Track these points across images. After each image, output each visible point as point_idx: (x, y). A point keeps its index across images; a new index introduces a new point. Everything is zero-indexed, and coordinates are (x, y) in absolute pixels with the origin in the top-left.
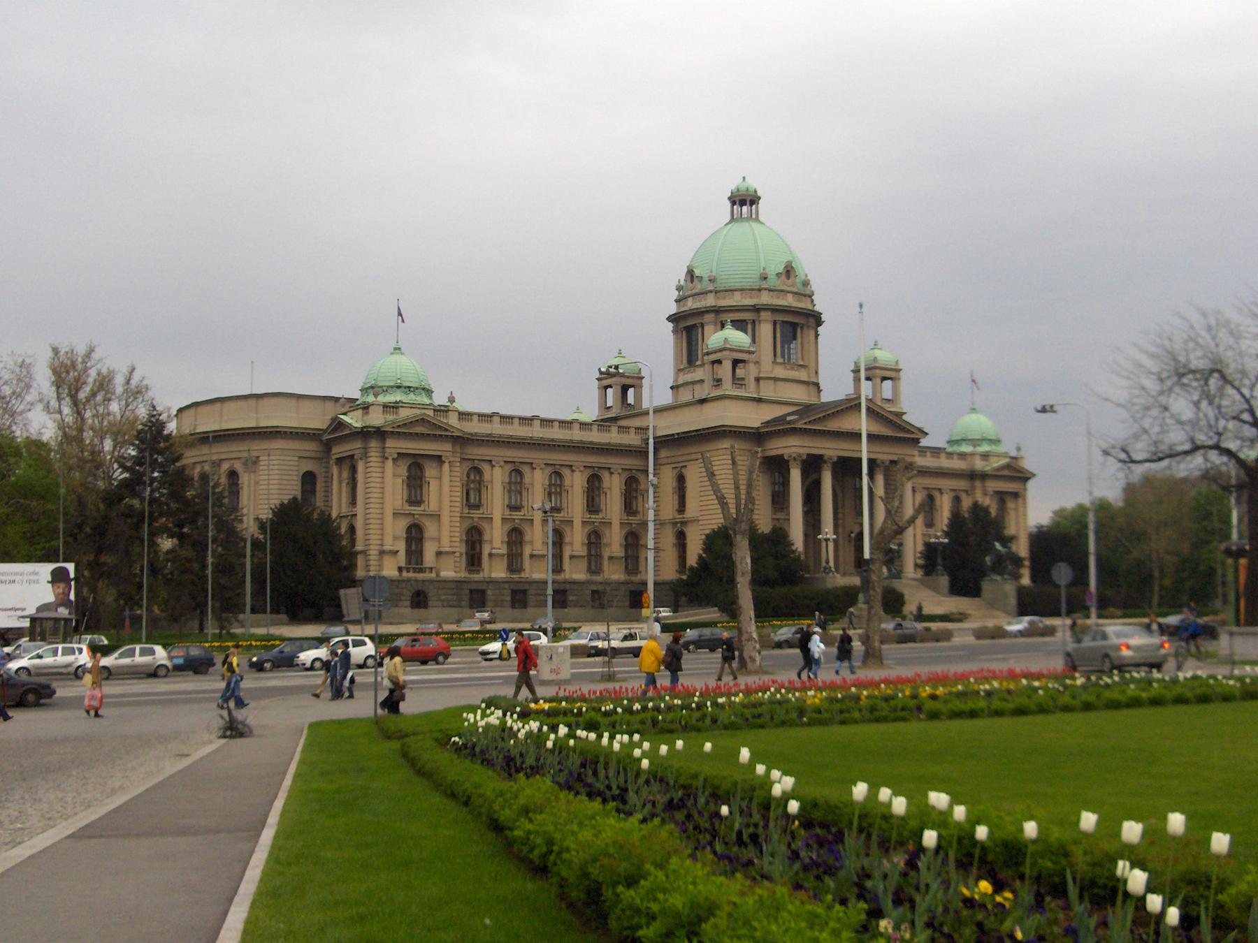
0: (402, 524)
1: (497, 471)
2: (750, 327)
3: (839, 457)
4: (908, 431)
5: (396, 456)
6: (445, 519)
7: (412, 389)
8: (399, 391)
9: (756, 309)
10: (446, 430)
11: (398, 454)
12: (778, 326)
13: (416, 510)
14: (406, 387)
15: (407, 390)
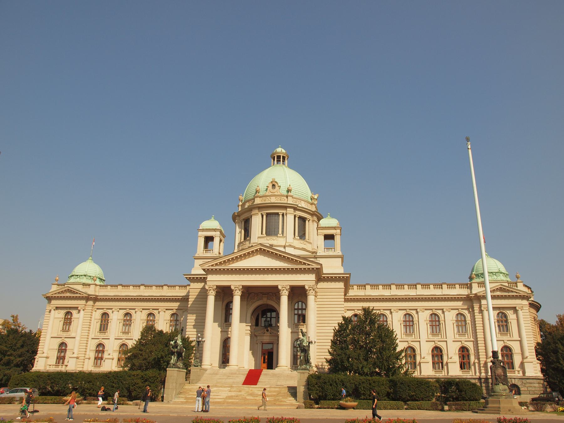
0: (56, 344)
1: (115, 313)
2: (250, 219)
3: (244, 287)
4: (305, 264)
5: (55, 308)
6: (78, 338)
7: (78, 276)
8: (73, 277)
9: (251, 209)
10: (79, 294)
11: (56, 307)
12: (265, 217)
13: (65, 334)
14: (76, 276)
15: (77, 276)
